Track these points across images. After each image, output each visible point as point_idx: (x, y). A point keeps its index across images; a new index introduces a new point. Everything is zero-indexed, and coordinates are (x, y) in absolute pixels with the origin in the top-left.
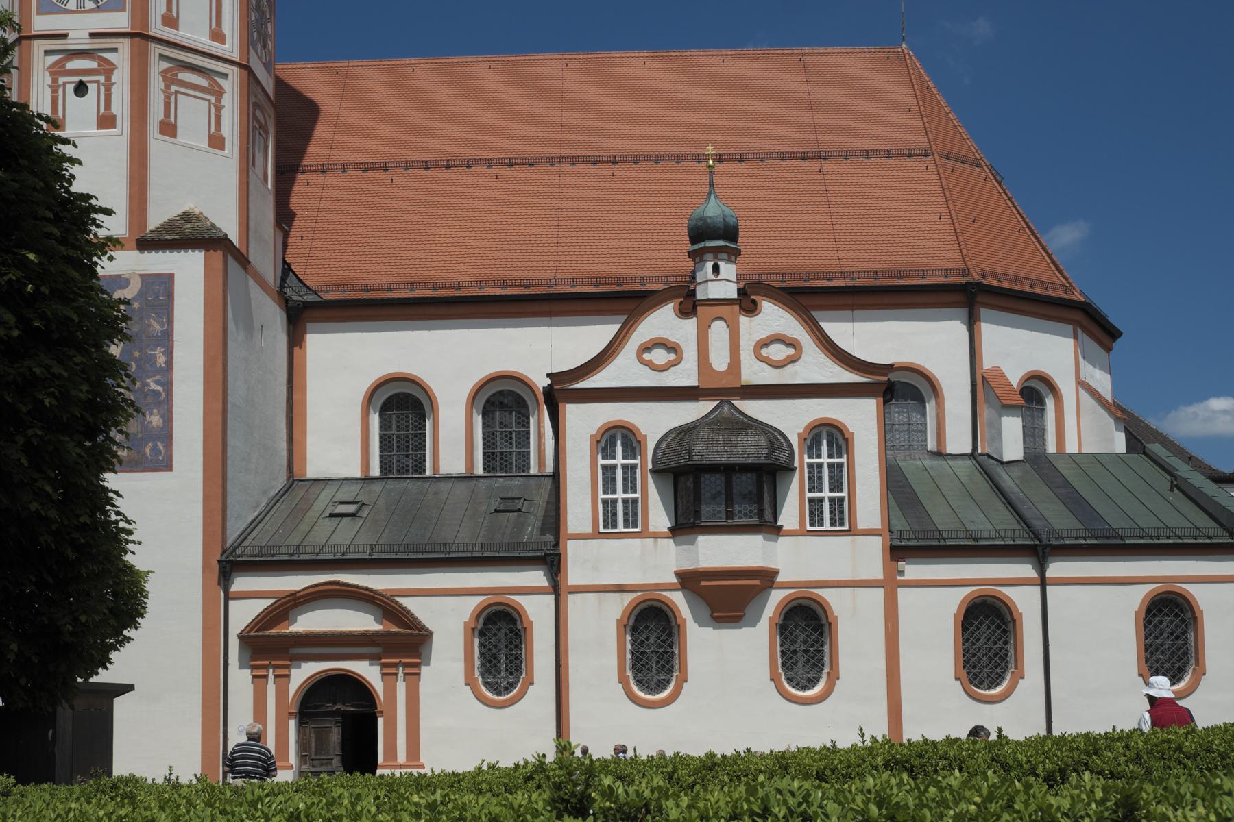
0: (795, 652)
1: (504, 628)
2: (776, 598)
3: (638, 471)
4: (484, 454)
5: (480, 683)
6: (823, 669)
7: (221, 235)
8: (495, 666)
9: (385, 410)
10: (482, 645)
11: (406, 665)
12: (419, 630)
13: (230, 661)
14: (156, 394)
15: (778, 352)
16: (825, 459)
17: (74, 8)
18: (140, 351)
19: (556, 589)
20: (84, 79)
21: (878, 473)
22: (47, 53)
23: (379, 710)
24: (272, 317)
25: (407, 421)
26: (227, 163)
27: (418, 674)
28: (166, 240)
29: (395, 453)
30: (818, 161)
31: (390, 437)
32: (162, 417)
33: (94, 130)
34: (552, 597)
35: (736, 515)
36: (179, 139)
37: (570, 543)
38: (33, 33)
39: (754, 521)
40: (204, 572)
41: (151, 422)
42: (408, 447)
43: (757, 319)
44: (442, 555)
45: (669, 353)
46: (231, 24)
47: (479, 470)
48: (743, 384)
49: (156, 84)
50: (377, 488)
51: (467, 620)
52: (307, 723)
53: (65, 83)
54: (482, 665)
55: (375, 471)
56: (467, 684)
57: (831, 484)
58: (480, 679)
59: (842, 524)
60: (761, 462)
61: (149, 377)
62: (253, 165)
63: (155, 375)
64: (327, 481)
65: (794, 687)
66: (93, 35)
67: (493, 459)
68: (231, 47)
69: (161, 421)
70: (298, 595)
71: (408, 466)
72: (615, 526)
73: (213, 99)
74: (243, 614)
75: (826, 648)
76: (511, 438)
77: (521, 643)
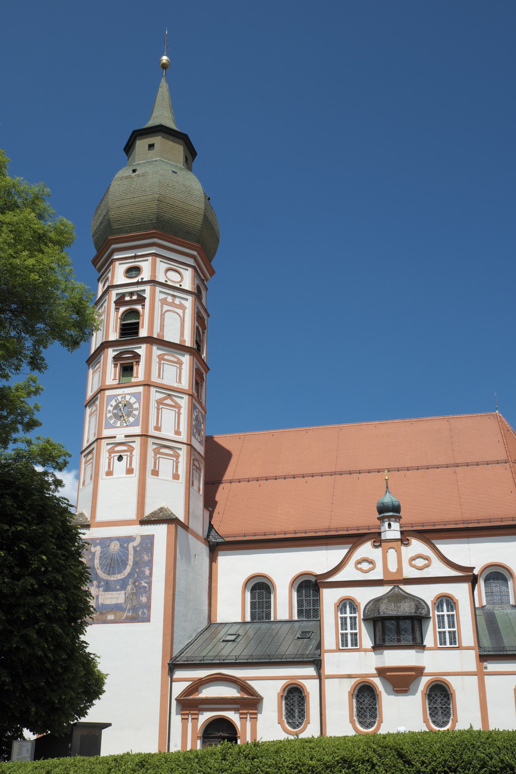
0: (436, 708)
1: (296, 695)
2: (424, 681)
3: (357, 620)
4: (298, 610)
5: (285, 723)
6: (450, 717)
7: (174, 517)
8: (292, 714)
9: (253, 589)
10: (286, 704)
11: (251, 714)
12: (257, 697)
13: (172, 711)
14: (145, 587)
15: (420, 562)
16: (445, 613)
17: (119, 426)
18: (139, 568)
19: (320, 676)
20: (121, 454)
21: (471, 619)
22: (108, 444)
23: (238, 736)
24: (203, 550)
25: (263, 595)
26: (180, 486)
27: (256, 718)
28: (152, 520)
29: (257, 610)
30: (454, 468)
31: (255, 603)
32: (147, 598)
33: (124, 475)
34: (318, 681)
35: (402, 640)
36: (160, 477)
37: (326, 654)
38: (103, 436)
39: (411, 643)
41: (142, 600)
42: (263, 607)
43: (409, 548)
44: (268, 661)
45: (369, 564)
46: (184, 428)
47: (295, 617)
48: (404, 578)
49: (150, 454)
50: (248, 626)
51: (279, 692)
52: (206, 742)
53: (114, 456)
54: (287, 714)
55: (248, 619)
56: (279, 723)
57: (449, 624)
58: (285, 720)
59: (455, 644)
60: (412, 615)
61: (142, 580)
62: (193, 485)
64: (226, 624)
65: (436, 726)
66: (126, 436)
67: (302, 612)
68: (183, 437)
69: (146, 599)
70: (203, 680)
71: (263, 616)
72: (347, 646)
73: (175, 459)
74: (178, 688)
75: (451, 706)
76: (310, 602)
77: (304, 703)
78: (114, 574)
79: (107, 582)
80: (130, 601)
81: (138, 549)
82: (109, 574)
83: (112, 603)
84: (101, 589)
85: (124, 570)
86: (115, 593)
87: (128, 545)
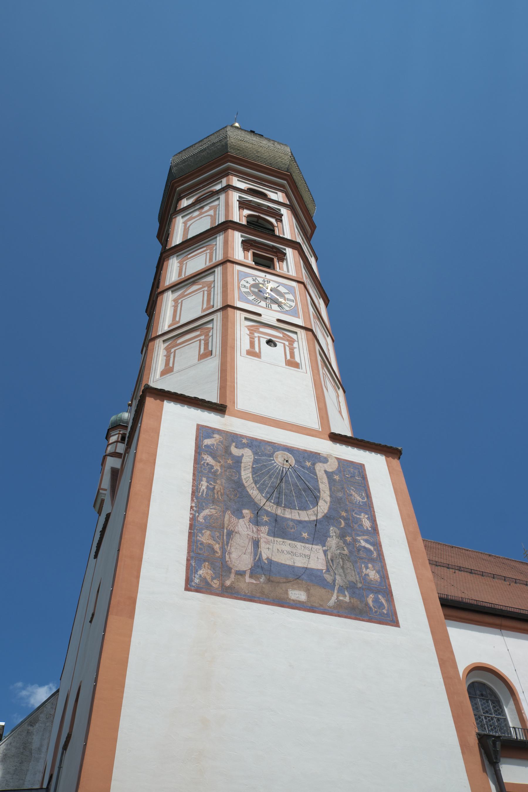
18: (346, 511)
40: (463, 753)
41: (368, 575)
63: (363, 535)
69: (378, 576)
78: (290, 506)
79: (276, 519)
80: (341, 571)
81: (337, 477)
82: (278, 504)
83: (296, 565)
84: (265, 529)
86: (299, 544)
87: (314, 464)
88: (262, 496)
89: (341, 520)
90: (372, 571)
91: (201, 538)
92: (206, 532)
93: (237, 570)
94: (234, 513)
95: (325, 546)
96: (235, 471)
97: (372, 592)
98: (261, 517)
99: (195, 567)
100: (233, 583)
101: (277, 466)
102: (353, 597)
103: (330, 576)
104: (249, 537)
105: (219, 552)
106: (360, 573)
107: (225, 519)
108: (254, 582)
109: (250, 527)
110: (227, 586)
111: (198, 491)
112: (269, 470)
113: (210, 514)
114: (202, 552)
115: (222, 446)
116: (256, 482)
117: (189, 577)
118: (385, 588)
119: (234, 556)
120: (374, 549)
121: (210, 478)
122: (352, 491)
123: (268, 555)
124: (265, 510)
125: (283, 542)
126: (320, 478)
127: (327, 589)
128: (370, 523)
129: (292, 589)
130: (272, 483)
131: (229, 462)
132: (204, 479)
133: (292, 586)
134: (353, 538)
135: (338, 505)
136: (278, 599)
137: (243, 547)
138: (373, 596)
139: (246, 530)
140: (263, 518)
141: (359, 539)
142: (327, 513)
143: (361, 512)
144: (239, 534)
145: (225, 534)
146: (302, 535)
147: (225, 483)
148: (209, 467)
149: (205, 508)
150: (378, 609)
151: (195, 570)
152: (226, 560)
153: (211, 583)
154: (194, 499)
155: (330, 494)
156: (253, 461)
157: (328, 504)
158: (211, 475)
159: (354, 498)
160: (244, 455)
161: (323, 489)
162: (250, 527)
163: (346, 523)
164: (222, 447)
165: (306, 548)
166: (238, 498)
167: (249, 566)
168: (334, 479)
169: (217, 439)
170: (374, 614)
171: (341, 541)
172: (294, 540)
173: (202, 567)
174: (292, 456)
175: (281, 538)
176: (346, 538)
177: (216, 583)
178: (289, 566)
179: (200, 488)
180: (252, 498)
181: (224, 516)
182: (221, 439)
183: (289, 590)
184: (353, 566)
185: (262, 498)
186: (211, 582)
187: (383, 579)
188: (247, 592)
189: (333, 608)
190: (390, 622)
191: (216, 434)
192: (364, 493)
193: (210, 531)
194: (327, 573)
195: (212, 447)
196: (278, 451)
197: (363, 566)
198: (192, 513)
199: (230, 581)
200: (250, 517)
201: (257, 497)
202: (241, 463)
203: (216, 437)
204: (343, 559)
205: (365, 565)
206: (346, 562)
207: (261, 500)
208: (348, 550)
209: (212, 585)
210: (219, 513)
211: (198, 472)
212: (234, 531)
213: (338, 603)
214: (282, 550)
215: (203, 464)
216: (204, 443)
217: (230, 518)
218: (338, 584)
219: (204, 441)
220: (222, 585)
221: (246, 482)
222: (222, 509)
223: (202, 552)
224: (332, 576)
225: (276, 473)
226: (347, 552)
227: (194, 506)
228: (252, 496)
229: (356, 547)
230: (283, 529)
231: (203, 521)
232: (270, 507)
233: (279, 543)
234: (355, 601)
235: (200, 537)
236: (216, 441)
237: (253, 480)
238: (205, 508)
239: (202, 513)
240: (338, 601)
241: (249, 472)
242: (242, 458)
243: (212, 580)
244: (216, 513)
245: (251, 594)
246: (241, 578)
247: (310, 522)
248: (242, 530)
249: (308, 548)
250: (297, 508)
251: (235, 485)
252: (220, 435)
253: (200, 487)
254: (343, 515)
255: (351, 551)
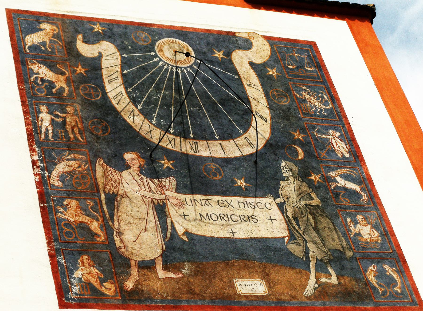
18: (302, 130)
41: (359, 234)
63: (339, 168)
69: (377, 234)
80: (315, 234)
81: (272, 72)
83: (237, 236)
85: (246, 130)
86: (234, 200)
87: (228, 54)
88: (152, 124)
89: (295, 146)
90: (364, 227)
91: (65, 215)
92: (69, 203)
93: (139, 260)
94: (109, 162)
95: (279, 197)
96: (93, 85)
97: (372, 262)
98: (159, 162)
99: (66, 265)
100: (137, 283)
101: (165, 67)
102: (342, 276)
103: (299, 246)
104: (147, 199)
105: (101, 234)
106: (347, 233)
107: (97, 174)
108: (174, 276)
109: (143, 183)
110: (129, 289)
111: (38, 132)
112: (153, 76)
113: (69, 170)
114: (72, 238)
115: (61, 44)
116: (135, 101)
117: (60, 284)
118: (391, 251)
119: (128, 236)
120: (362, 189)
121: (53, 104)
122: (304, 94)
123: (186, 227)
124: (163, 148)
125: (207, 200)
126: (245, 77)
127: (297, 269)
128: (346, 144)
129: (240, 278)
130: (164, 97)
131: (79, 71)
132: (43, 108)
133: (238, 273)
134: (322, 175)
135: (286, 122)
136: (220, 299)
137: (140, 219)
138: (375, 268)
139: (137, 188)
140: (161, 163)
141: (333, 175)
142: (270, 138)
143: (327, 128)
144: (128, 197)
145: (104, 202)
146: (236, 183)
147: (81, 111)
148: (46, 86)
149: (58, 161)
150: (386, 288)
151: (67, 271)
152: (117, 246)
153: (101, 289)
154: (34, 147)
155: (268, 103)
156: (122, 62)
157: (269, 122)
158: (52, 99)
159: (311, 105)
160: (103, 53)
161: (255, 97)
162: (143, 183)
163: (306, 151)
164: (61, 46)
165: (247, 205)
166: (110, 134)
167: (158, 251)
168: (269, 75)
169: (49, 33)
170: (382, 297)
171: (304, 184)
172: (224, 194)
173: (79, 264)
174: (188, 44)
175: (201, 194)
176: (312, 178)
177: (109, 287)
178: (226, 240)
179: (41, 126)
180: (135, 130)
181: (94, 170)
182: (55, 30)
183: (234, 280)
184: (333, 223)
185: (153, 127)
186: (101, 288)
187: (385, 237)
188: (165, 295)
189: (314, 299)
190: (409, 306)
191: (44, 22)
192: (326, 95)
193: (77, 199)
194: (292, 242)
195: (43, 48)
196: (160, 39)
197: (349, 220)
198: (37, 173)
199: (132, 281)
200: (138, 164)
201: (142, 127)
202: (101, 69)
203: (45, 29)
204: (314, 214)
205: (352, 219)
206: (320, 217)
207: (150, 132)
208: (318, 198)
209: (104, 292)
210: (84, 166)
211: (30, 98)
212: (118, 193)
213: (320, 288)
214: (207, 214)
215: (35, 82)
216: (26, 42)
217: (106, 172)
218: (314, 258)
219: (26, 39)
220: (121, 289)
221: (117, 104)
222: (87, 158)
223: (72, 238)
224: (301, 246)
225: (166, 79)
226: (317, 201)
227: (37, 160)
228: (133, 126)
229: (331, 190)
230: (202, 178)
231: (61, 184)
232: (170, 142)
233: (200, 202)
234: (346, 280)
235: (61, 212)
236: (46, 35)
237: (129, 97)
238: (58, 161)
239: (54, 170)
240: (319, 286)
241: (119, 84)
242: (101, 61)
243: (101, 285)
244: (78, 167)
245: (173, 297)
246: (150, 274)
247: (244, 158)
248: (131, 190)
249: (251, 203)
250: (218, 137)
251: (100, 112)
252: (52, 23)
253: (40, 123)
254: (298, 138)
255: (324, 198)
